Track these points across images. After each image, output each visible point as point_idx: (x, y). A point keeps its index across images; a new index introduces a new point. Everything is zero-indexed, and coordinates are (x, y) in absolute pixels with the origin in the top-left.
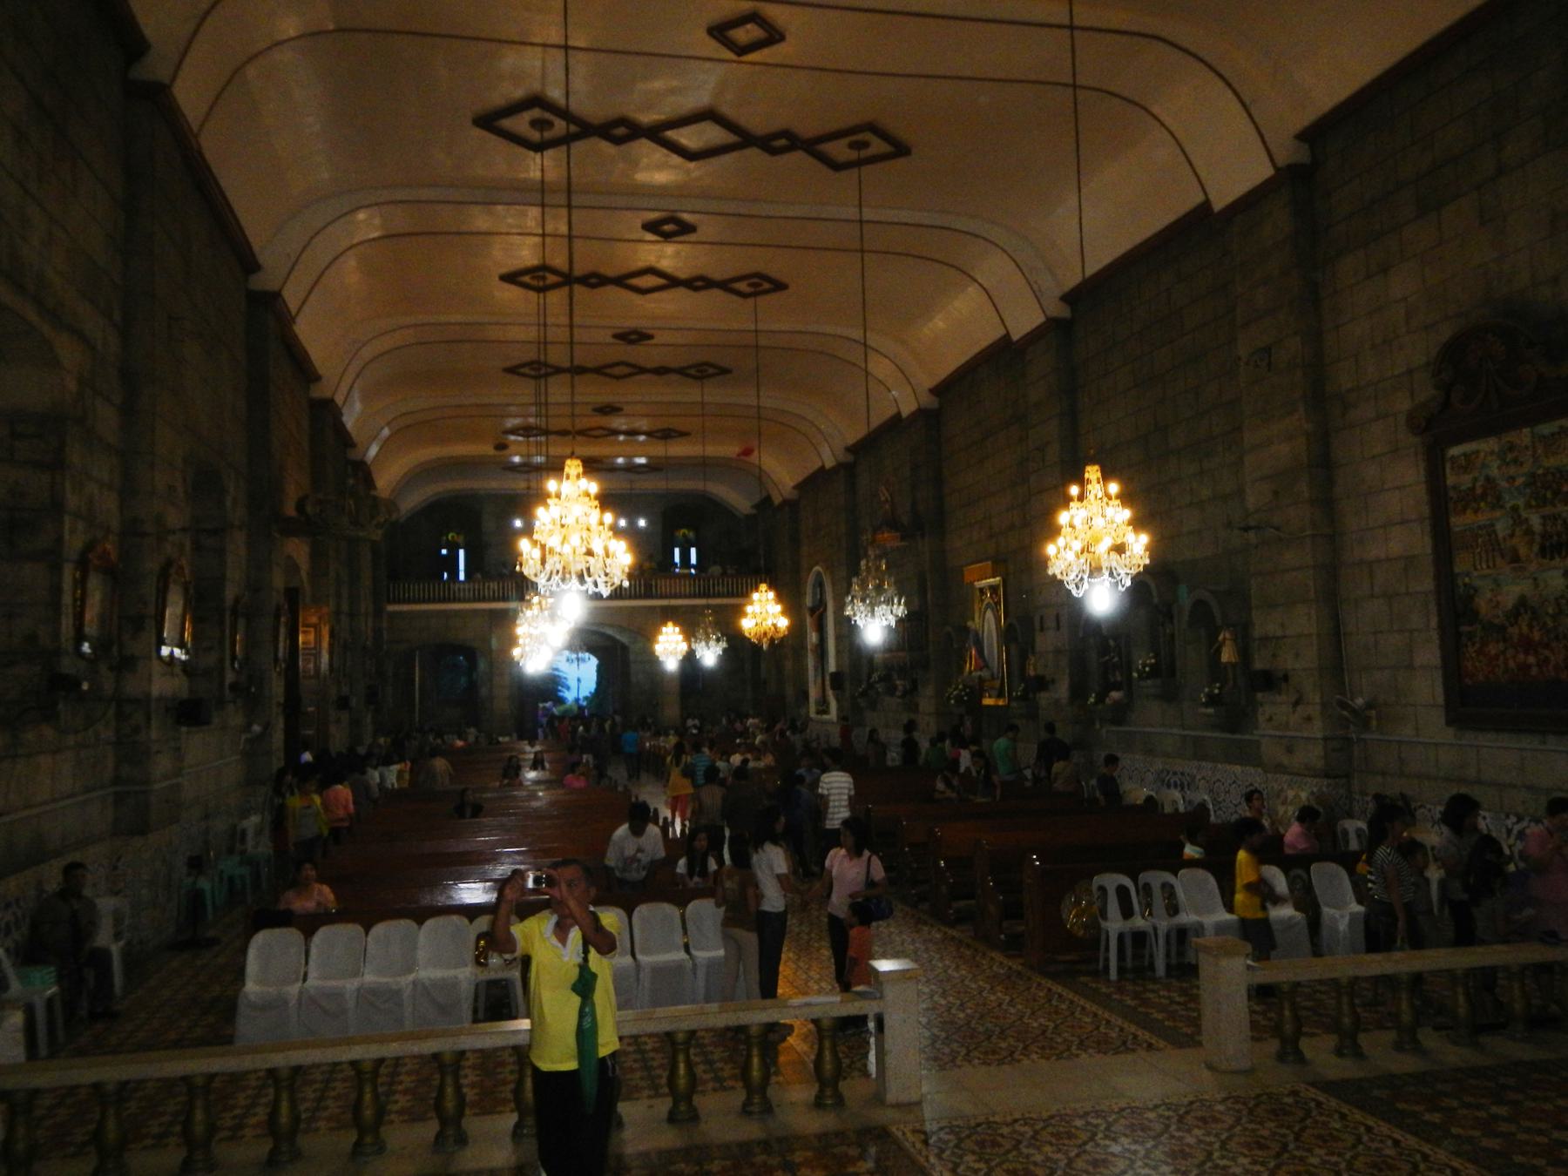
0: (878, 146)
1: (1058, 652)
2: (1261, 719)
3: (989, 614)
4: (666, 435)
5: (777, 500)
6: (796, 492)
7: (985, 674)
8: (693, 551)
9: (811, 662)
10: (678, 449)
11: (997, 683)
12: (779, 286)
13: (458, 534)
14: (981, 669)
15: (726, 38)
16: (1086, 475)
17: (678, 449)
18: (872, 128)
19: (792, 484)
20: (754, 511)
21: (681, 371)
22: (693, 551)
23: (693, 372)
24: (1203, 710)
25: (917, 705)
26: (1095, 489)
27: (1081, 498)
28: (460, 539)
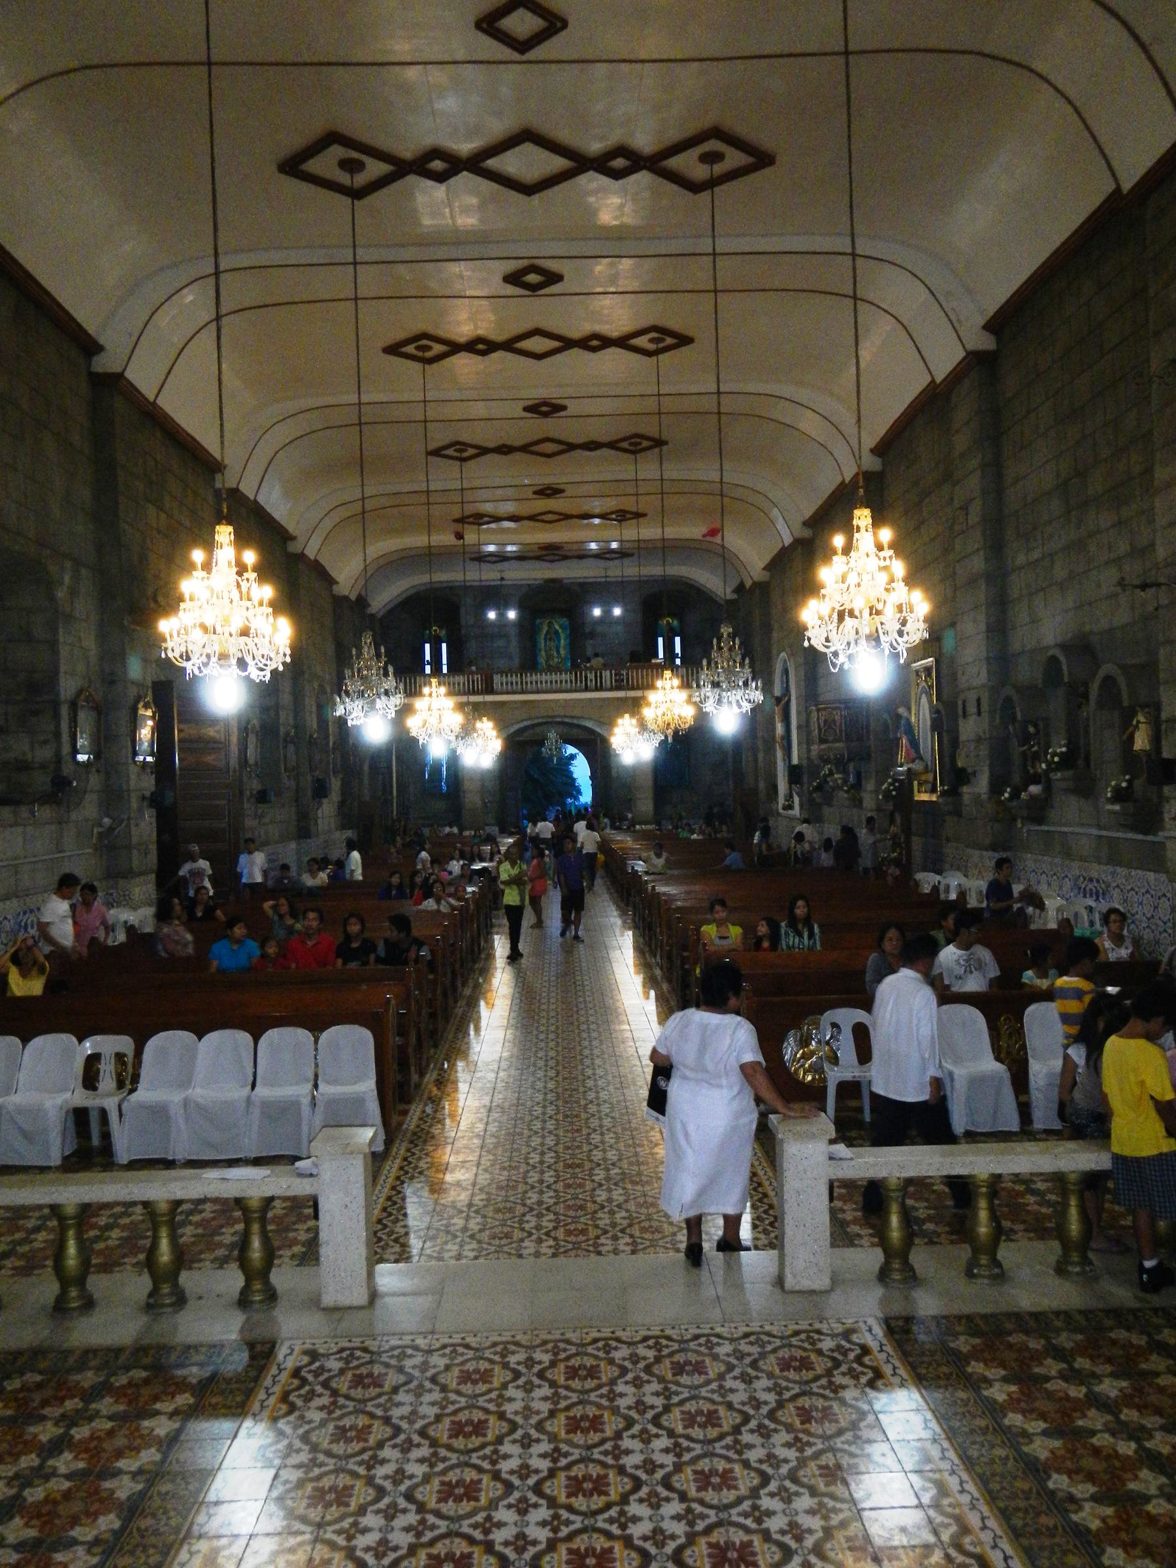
0: (734, 159)
1: (979, 740)
2: (1166, 817)
3: (924, 699)
4: (622, 516)
5: (748, 584)
6: (767, 574)
7: (917, 766)
8: (678, 640)
9: (779, 754)
10: (649, 531)
11: (930, 777)
12: (684, 340)
14: (913, 761)
15: (498, 30)
16: (855, 522)
17: (631, 532)
18: (716, 133)
19: (762, 565)
20: (735, 596)
21: (612, 445)
22: (678, 640)
23: (625, 445)
24: (1109, 807)
25: (861, 801)
26: (865, 539)
27: (847, 550)
28: (443, 633)
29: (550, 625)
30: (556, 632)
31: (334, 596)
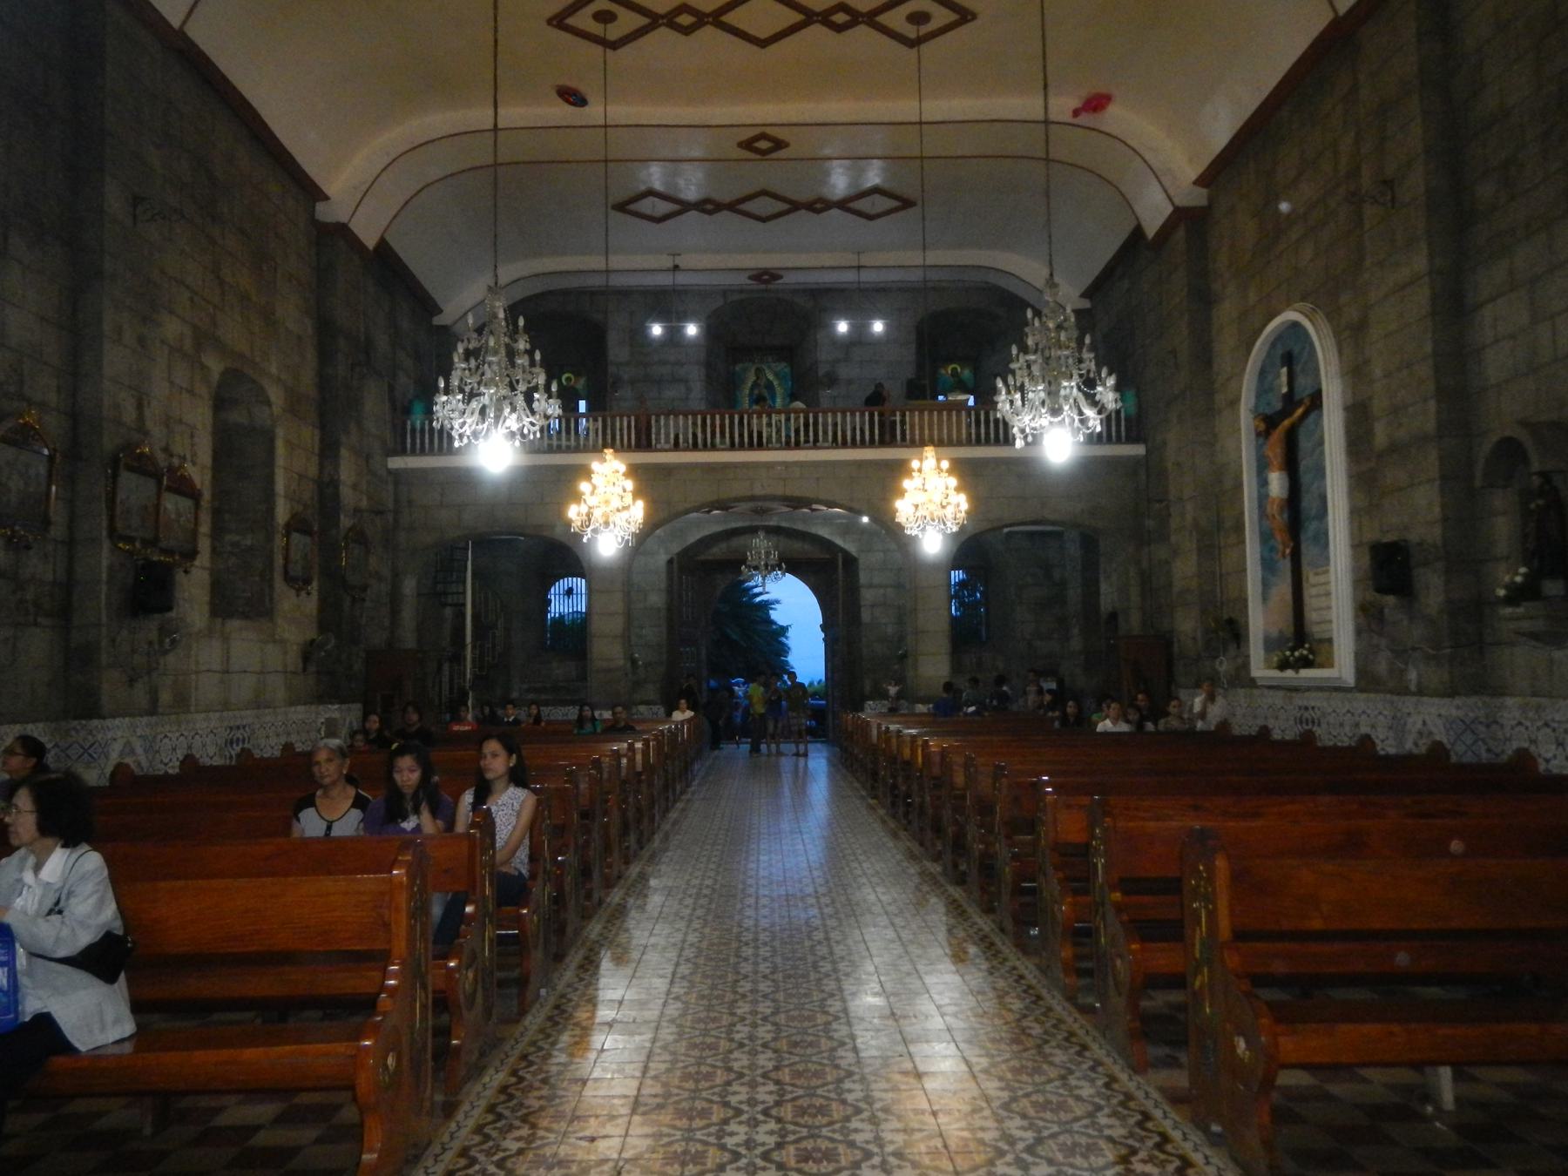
6: (1204, 191)
13: (578, 374)
19: (1193, 173)
28: (581, 384)
29: (759, 371)
30: (770, 386)
31: (314, 222)
